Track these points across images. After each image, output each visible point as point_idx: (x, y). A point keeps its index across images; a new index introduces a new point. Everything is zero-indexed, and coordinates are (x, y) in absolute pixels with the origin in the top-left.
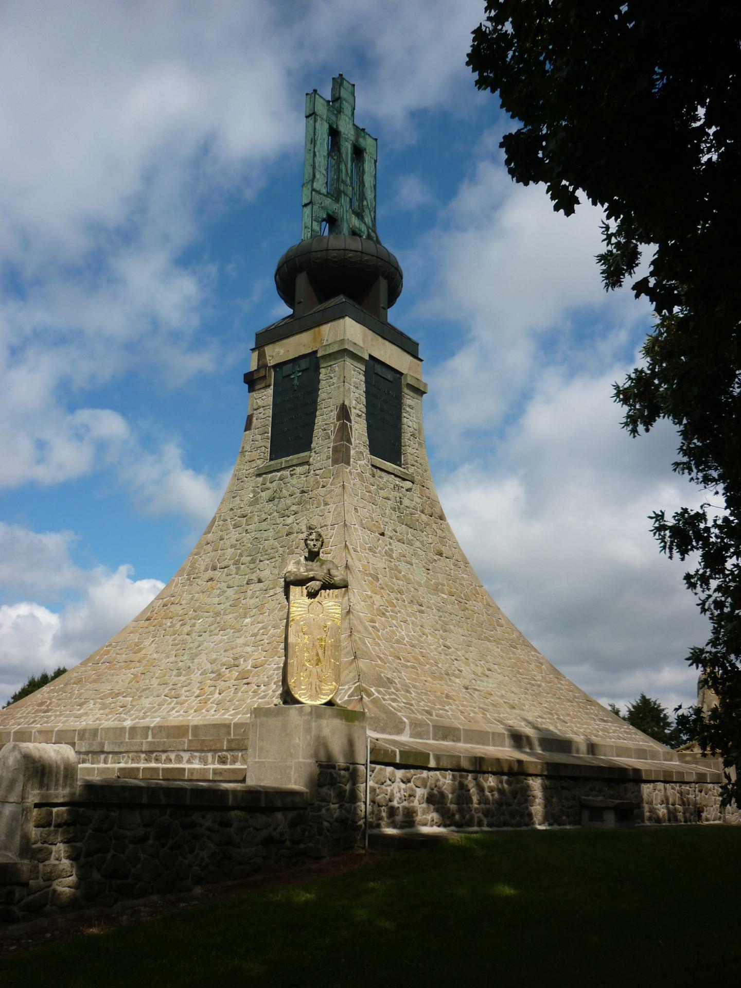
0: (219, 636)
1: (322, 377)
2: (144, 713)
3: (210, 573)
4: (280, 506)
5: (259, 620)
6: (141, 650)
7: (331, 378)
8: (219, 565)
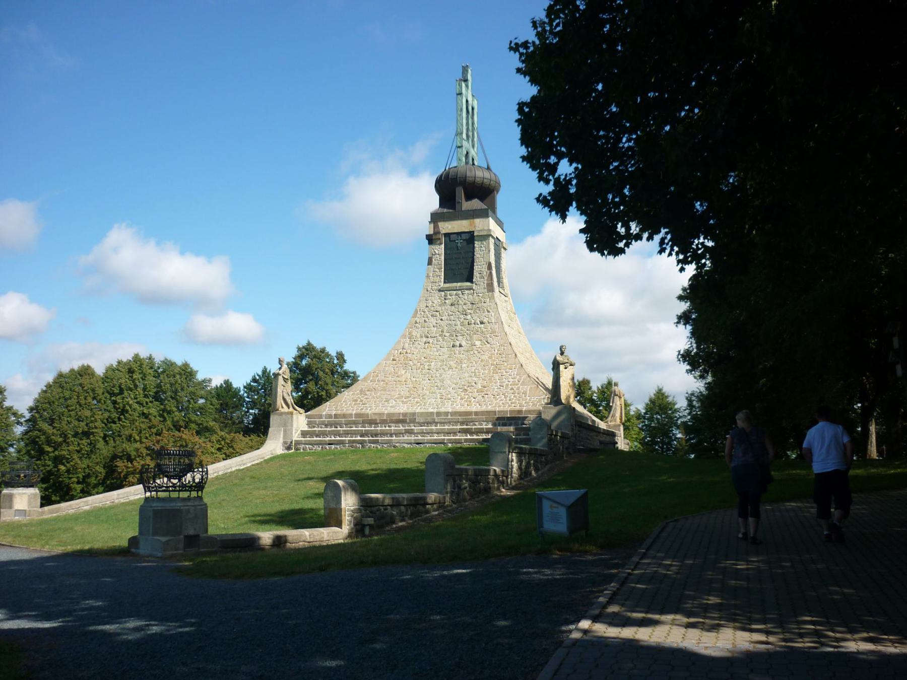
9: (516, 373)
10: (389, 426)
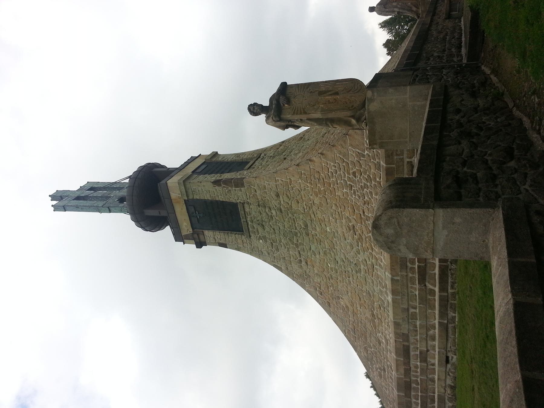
0: (337, 248)
1: (198, 198)
2: (383, 288)
3: (303, 263)
4: (266, 220)
5: (328, 220)
6: (347, 307)
7: (199, 191)
8: (299, 259)
9: (332, 164)
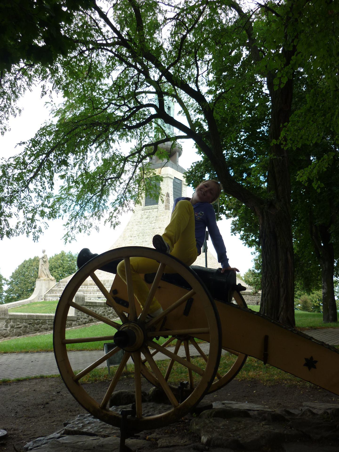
3: (131, 238)
4: (150, 220)
10: (94, 288)
